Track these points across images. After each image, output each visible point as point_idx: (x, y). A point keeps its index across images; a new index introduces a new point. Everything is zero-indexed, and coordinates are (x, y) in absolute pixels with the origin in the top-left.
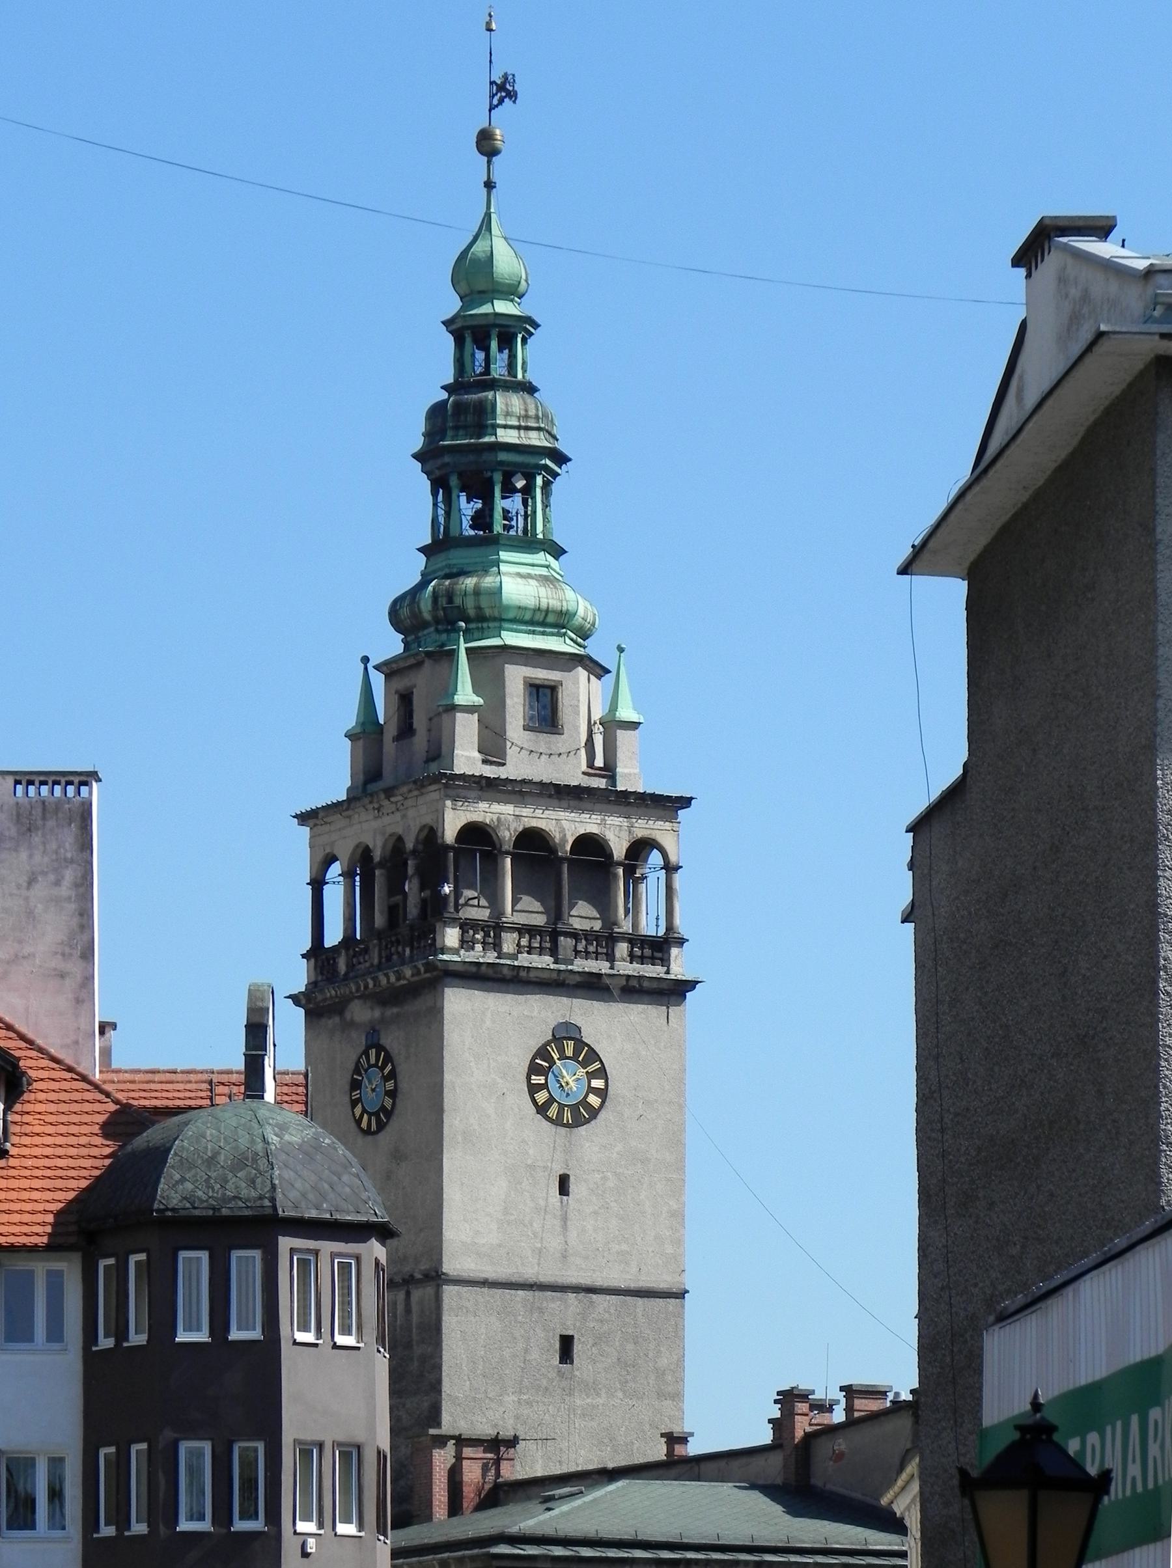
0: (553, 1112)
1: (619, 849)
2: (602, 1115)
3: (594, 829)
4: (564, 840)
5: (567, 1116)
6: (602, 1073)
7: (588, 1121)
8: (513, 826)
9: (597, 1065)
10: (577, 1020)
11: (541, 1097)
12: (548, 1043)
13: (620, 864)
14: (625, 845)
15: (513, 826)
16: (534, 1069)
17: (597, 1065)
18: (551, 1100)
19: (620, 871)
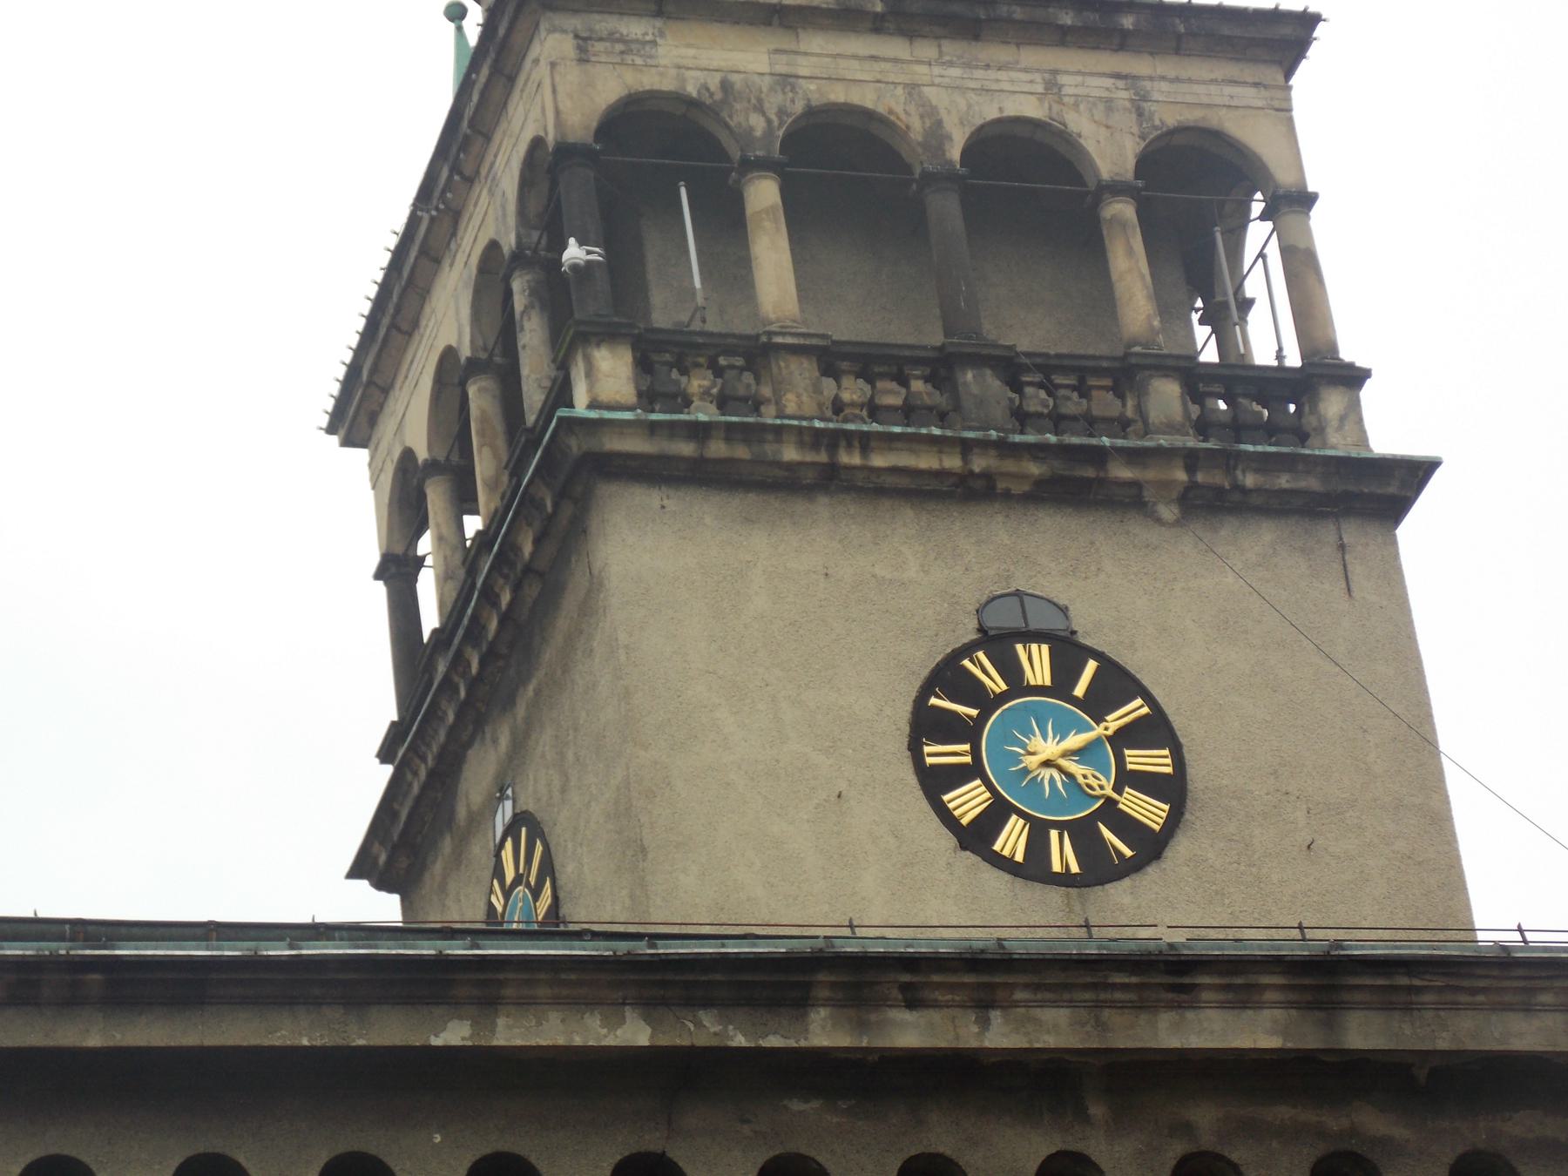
0: (1012, 839)
1: (1111, 150)
2: (1180, 848)
3: (1031, 109)
4: (937, 136)
5: (1063, 855)
8: (773, 103)
9: (1136, 708)
10: (1053, 586)
11: (968, 801)
12: (967, 650)
13: (1116, 189)
15: (773, 103)
16: (927, 725)
17: (1136, 708)
18: (997, 813)
19: (1123, 210)
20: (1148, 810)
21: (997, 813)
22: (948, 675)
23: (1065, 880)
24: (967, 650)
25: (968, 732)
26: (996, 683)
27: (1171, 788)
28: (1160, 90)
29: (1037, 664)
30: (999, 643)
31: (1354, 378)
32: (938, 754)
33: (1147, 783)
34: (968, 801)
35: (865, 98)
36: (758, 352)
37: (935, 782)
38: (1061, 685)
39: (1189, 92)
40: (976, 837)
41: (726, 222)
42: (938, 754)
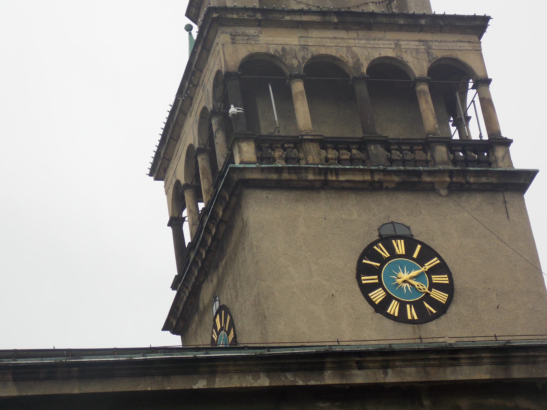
0: (394, 308)
1: (419, 67)
2: (453, 309)
3: (390, 53)
4: (358, 64)
5: (411, 313)
6: (442, 268)
7: (435, 317)
8: (300, 55)
9: (435, 261)
11: (378, 296)
12: (375, 243)
13: (421, 80)
14: (425, 66)
15: (300, 55)
16: (362, 270)
17: (435, 261)
18: (388, 300)
19: (424, 87)
20: (441, 296)
21: (388, 300)
22: (369, 252)
23: (413, 322)
24: (375, 243)
25: (377, 271)
26: (386, 254)
27: (448, 289)
28: (435, 45)
29: (400, 247)
30: (386, 240)
31: (507, 143)
32: (367, 280)
33: (440, 287)
34: (378, 296)
35: (332, 52)
36: (298, 142)
37: (366, 289)
38: (409, 254)
39: (445, 46)
40: (381, 308)
41: (285, 98)
42: (367, 280)
